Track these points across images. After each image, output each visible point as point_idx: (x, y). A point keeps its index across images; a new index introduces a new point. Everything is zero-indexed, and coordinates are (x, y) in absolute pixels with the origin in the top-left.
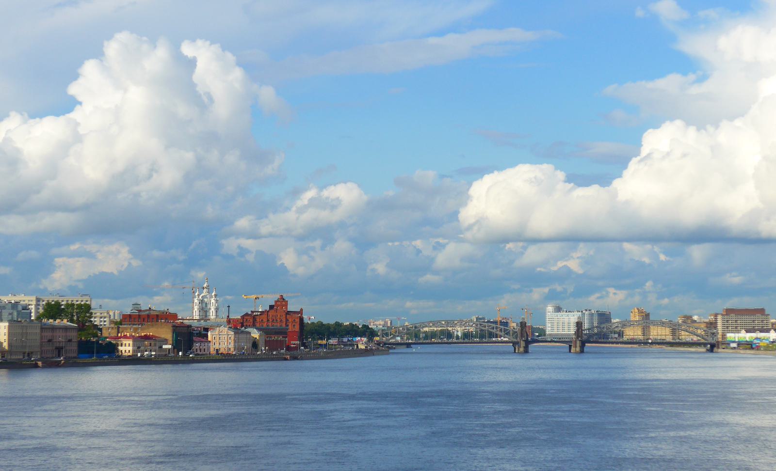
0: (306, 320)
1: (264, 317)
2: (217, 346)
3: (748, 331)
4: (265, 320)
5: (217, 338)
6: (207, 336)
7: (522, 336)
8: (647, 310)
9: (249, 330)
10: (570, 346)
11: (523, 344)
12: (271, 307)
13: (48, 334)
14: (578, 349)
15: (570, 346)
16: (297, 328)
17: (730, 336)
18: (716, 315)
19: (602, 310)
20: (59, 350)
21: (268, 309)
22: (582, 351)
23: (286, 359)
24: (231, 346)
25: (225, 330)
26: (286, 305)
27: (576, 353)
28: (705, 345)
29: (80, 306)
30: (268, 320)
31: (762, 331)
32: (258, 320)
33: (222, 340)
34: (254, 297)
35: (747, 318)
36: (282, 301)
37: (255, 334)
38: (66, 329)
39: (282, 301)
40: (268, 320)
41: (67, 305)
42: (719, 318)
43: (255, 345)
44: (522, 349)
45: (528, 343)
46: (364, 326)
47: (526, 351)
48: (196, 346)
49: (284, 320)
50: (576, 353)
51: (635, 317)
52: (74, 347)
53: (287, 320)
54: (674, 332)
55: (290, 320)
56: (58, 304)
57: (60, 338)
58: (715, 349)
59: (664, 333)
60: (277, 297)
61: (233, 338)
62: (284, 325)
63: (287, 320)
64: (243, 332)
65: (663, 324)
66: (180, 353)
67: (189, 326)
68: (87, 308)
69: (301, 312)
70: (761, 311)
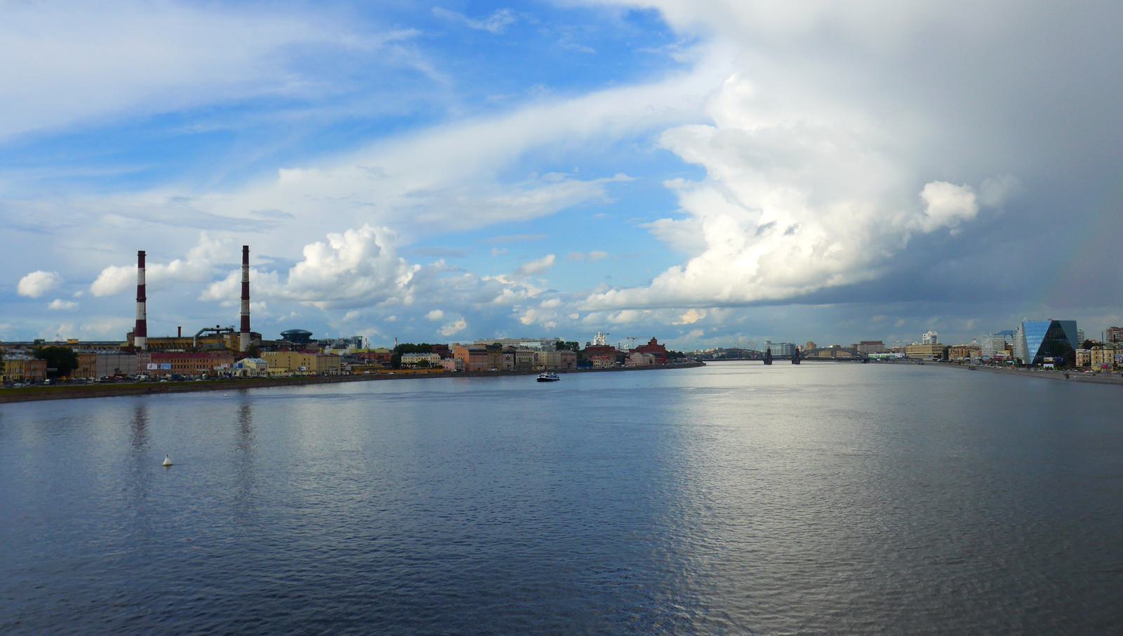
6: (629, 357)
13: (564, 357)
20: (569, 364)
21: (647, 344)
29: (573, 343)
35: (873, 346)
36: (654, 340)
38: (572, 354)
39: (654, 340)
41: (567, 343)
46: (680, 352)
52: (576, 364)
54: (832, 355)
56: (562, 342)
57: (569, 358)
59: (828, 354)
60: (652, 338)
68: (576, 344)
70: (880, 343)
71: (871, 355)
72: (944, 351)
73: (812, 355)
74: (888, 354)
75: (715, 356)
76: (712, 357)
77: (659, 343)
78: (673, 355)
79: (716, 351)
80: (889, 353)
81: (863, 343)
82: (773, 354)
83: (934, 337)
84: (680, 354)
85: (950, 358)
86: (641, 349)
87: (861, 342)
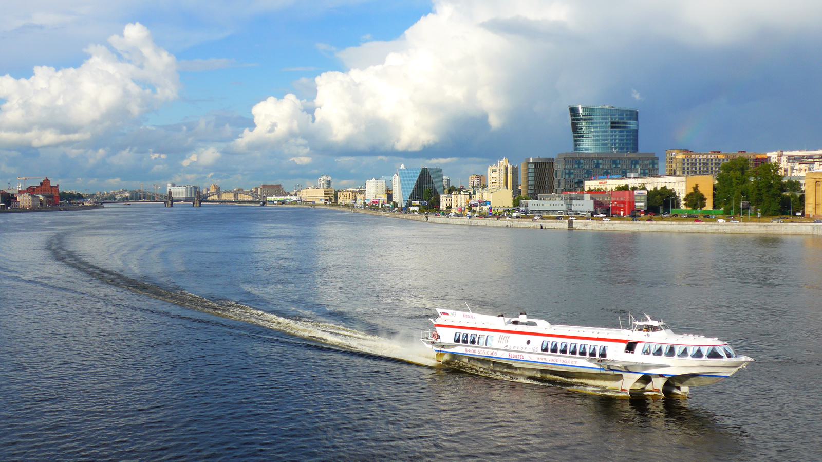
0: (60, 191)
1: (39, 189)
2: (22, 205)
3: (276, 196)
4: (39, 190)
5: (22, 200)
6: (16, 199)
7: (169, 198)
8: (218, 185)
9: (37, 195)
10: (194, 204)
11: (170, 202)
12: (41, 184)
14: (198, 205)
15: (194, 204)
16: (57, 195)
17: (269, 198)
18: (257, 189)
19: (197, 185)
21: (39, 185)
22: (200, 206)
23: (61, 210)
24: (31, 203)
25: (26, 195)
26: (49, 183)
27: (197, 207)
28: (259, 202)
30: (41, 191)
31: (283, 196)
32: (36, 190)
33: (25, 200)
34: (24, 178)
35: (273, 190)
37: (41, 198)
39: (47, 181)
40: (41, 191)
42: (259, 189)
43: (41, 203)
44: (169, 205)
45: (173, 201)
47: (172, 206)
48: (13, 205)
49: (50, 190)
50: (197, 207)
51: (213, 190)
53: (52, 191)
55: (53, 190)
58: (265, 205)
61: (31, 200)
62: (50, 193)
63: (52, 191)
64: (35, 197)
65: (228, 192)
66: (9, 208)
67: (9, 194)
69: (57, 186)
71: (270, 198)
72: (334, 195)
73: (215, 197)
74: (285, 198)
75: (118, 197)
76: (115, 199)
77: (53, 184)
78: (71, 196)
79: (120, 193)
80: (287, 196)
81: (264, 186)
82: (174, 196)
83: (329, 182)
84: (79, 197)
85: (340, 201)
86: (31, 191)
87: (263, 186)
